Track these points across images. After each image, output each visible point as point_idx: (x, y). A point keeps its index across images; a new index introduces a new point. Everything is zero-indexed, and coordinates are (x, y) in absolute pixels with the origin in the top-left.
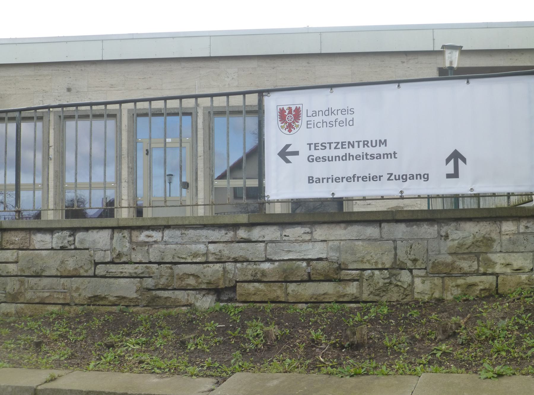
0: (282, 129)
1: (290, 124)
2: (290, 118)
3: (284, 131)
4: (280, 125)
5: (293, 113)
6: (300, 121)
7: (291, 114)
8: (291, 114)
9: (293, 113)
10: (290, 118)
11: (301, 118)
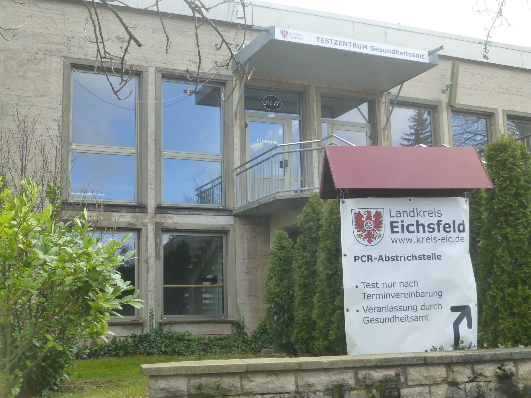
0: (359, 239)
1: (369, 232)
2: (369, 225)
3: (361, 241)
4: (356, 233)
5: (373, 219)
6: (382, 229)
7: (371, 219)
8: (371, 219)
9: (373, 219)
10: (369, 225)
11: (383, 226)
